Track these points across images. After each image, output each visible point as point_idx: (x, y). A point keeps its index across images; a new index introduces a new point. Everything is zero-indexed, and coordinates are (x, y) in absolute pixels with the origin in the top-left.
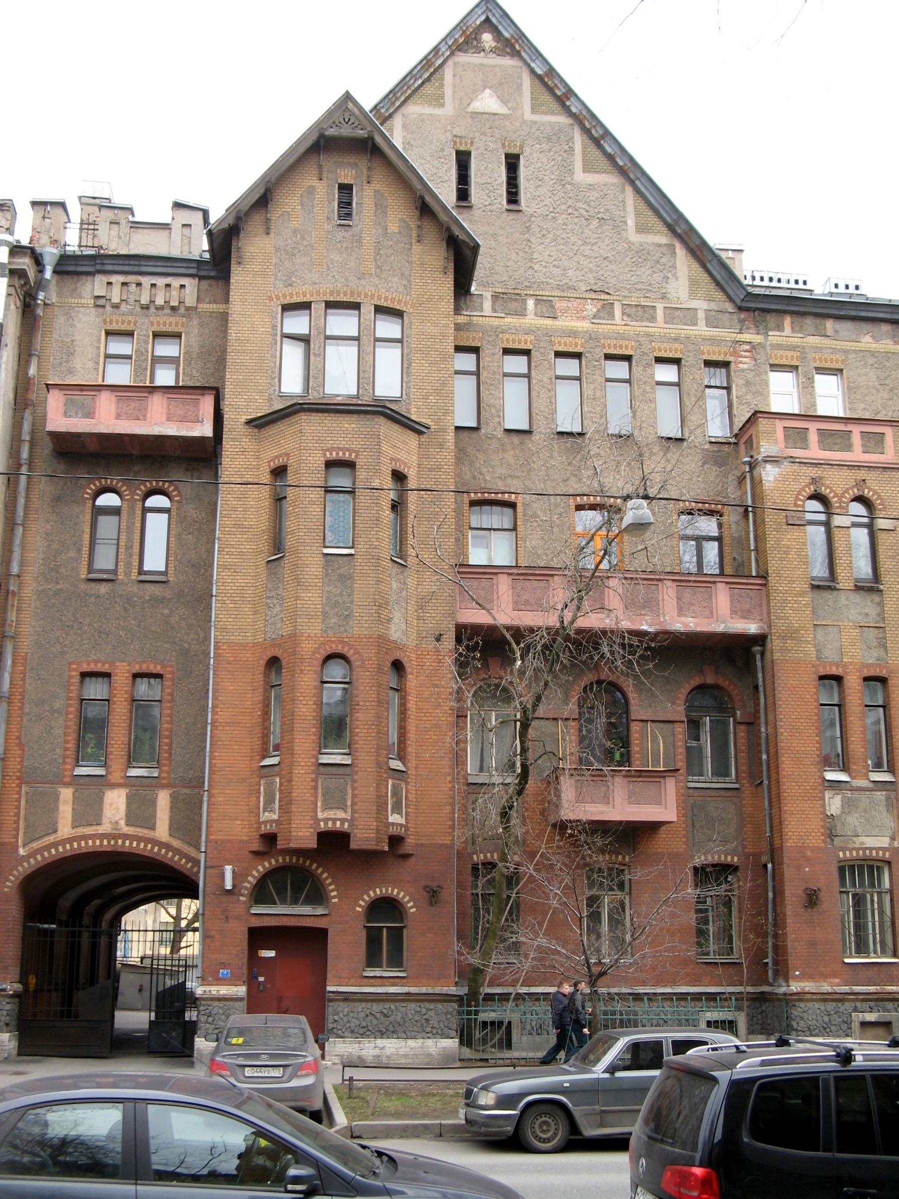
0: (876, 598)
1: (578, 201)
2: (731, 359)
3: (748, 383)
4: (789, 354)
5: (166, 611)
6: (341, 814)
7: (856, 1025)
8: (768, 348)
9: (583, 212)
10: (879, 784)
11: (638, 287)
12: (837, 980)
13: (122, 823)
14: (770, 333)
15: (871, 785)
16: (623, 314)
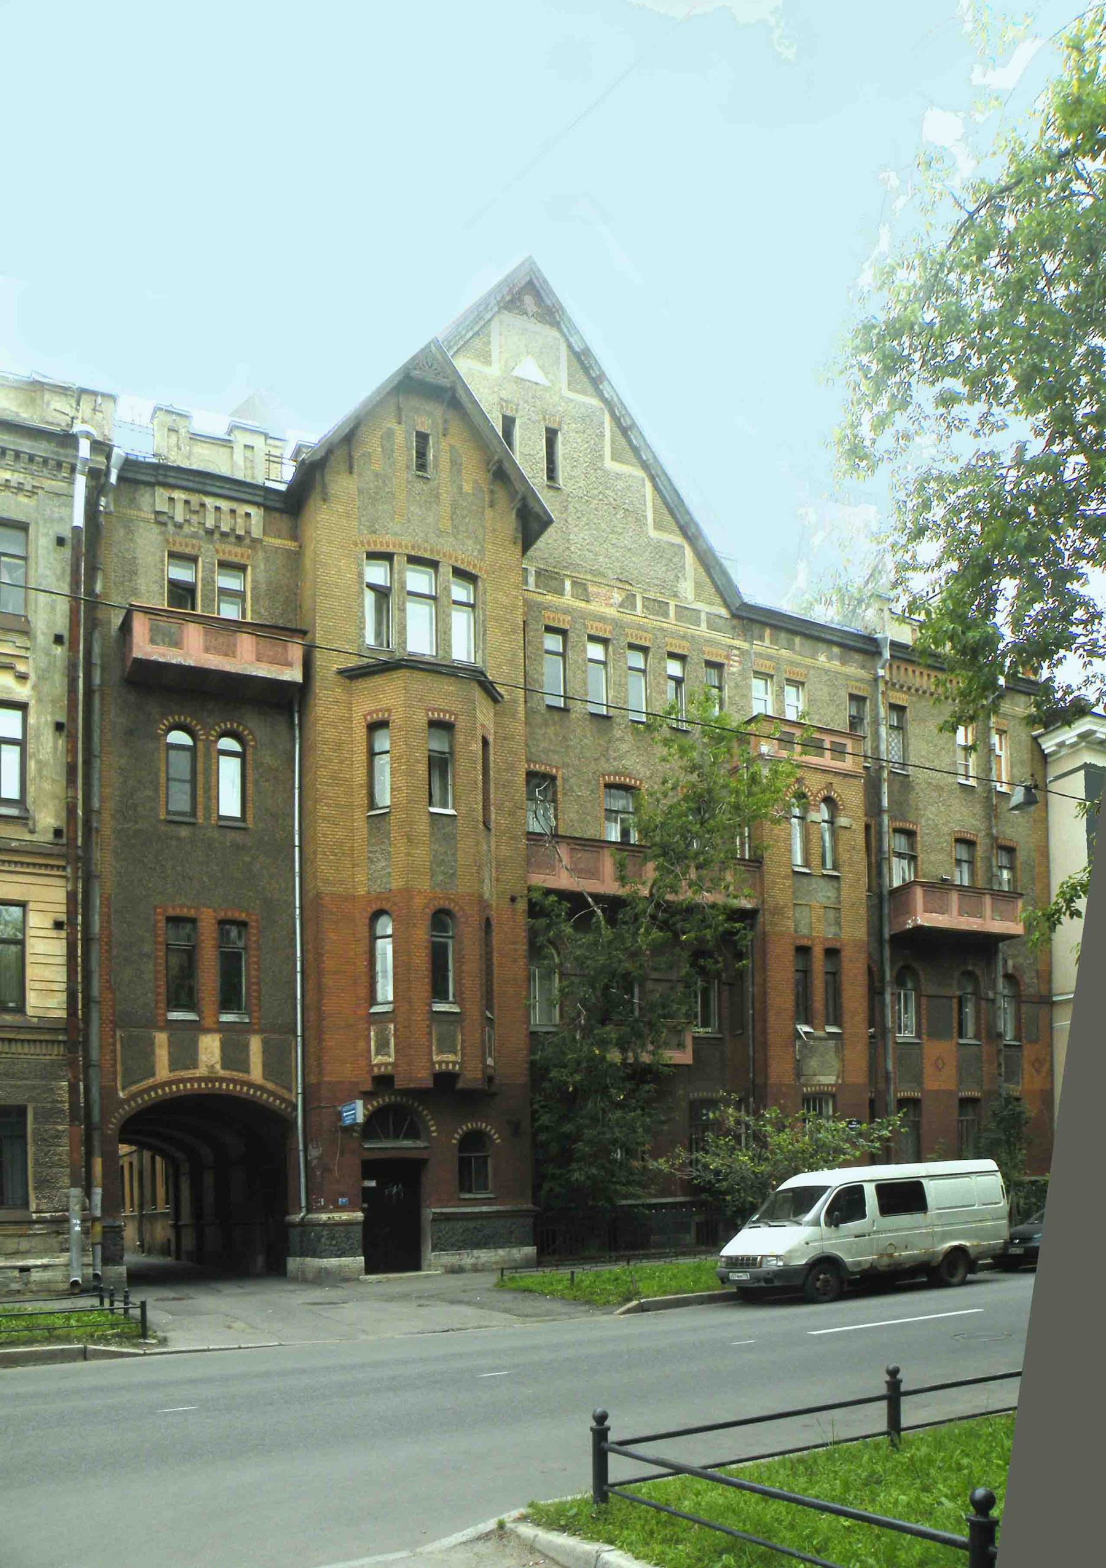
0: (836, 884)
2: (725, 661)
4: (768, 663)
5: (247, 859)
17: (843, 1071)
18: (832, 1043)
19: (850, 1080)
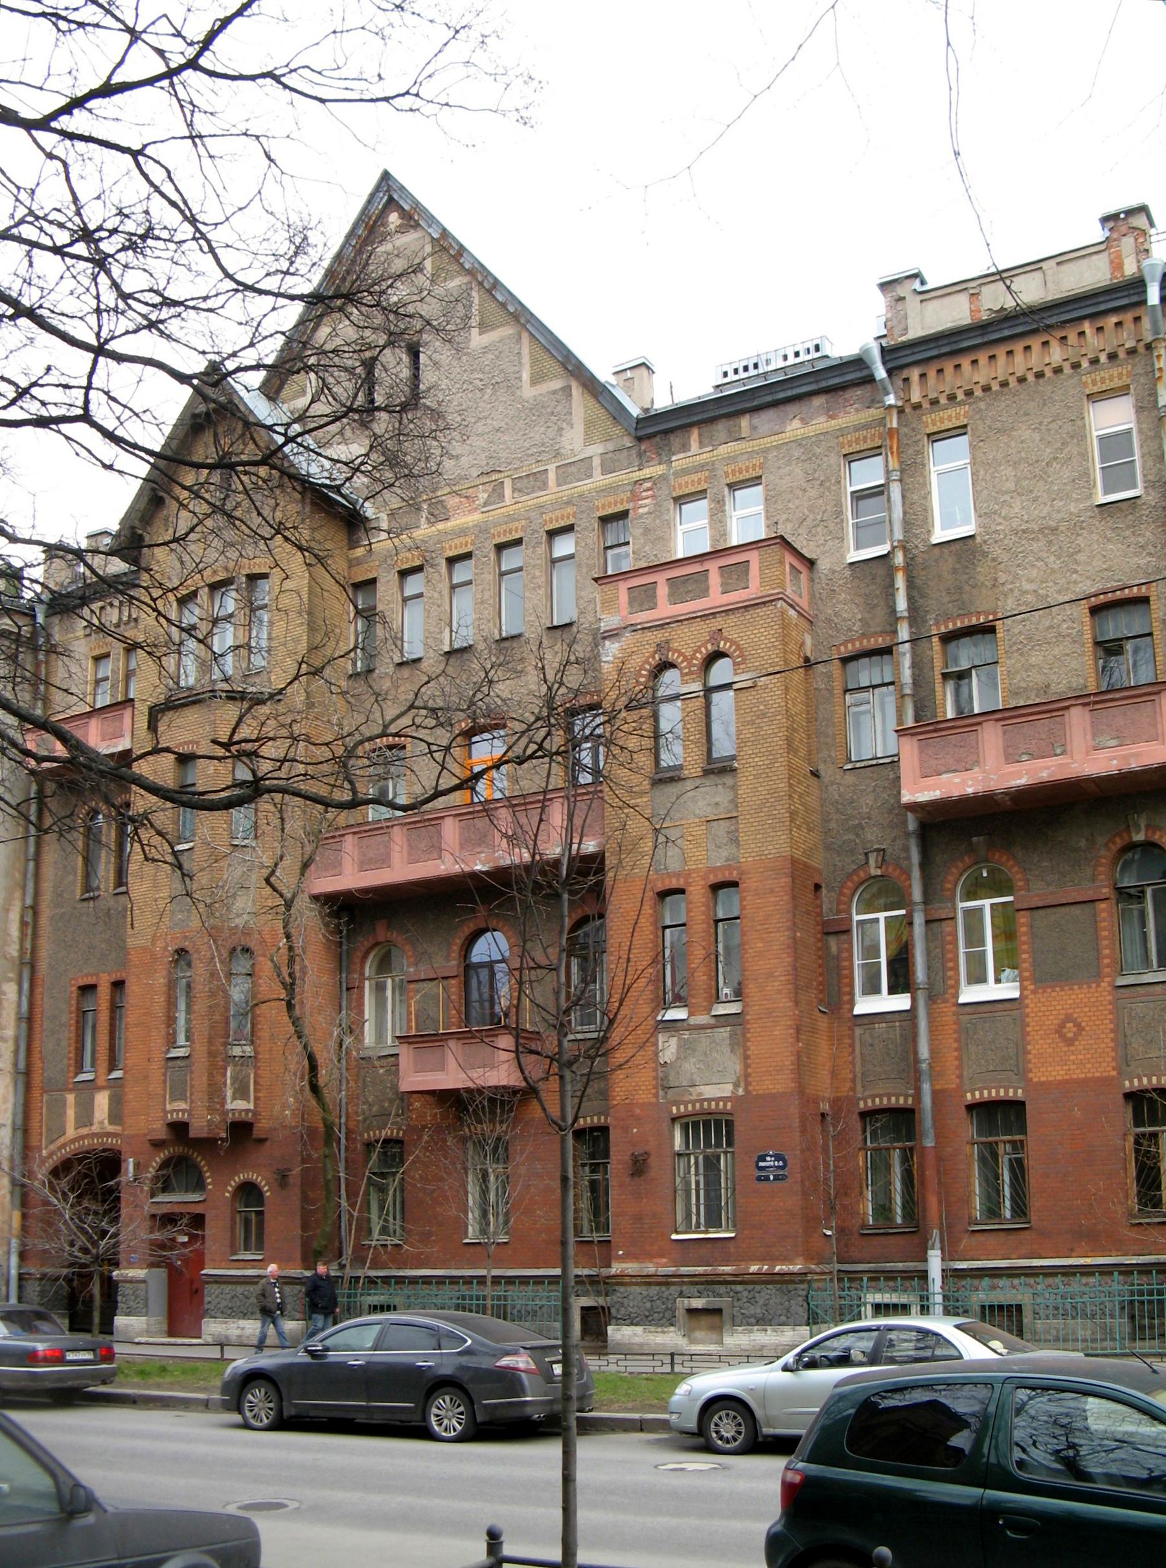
1: (472, 371)
3: (647, 531)
4: (695, 477)
6: (183, 1105)
7: (680, 1313)
8: (672, 477)
9: (477, 382)
10: (722, 1019)
11: (530, 452)
12: (664, 1260)
13: (106, 1122)
14: (674, 458)
15: (713, 1021)
16: (514, 490)
17: (747, 1076)
18: (724, 1033)
19: (757, 1088)
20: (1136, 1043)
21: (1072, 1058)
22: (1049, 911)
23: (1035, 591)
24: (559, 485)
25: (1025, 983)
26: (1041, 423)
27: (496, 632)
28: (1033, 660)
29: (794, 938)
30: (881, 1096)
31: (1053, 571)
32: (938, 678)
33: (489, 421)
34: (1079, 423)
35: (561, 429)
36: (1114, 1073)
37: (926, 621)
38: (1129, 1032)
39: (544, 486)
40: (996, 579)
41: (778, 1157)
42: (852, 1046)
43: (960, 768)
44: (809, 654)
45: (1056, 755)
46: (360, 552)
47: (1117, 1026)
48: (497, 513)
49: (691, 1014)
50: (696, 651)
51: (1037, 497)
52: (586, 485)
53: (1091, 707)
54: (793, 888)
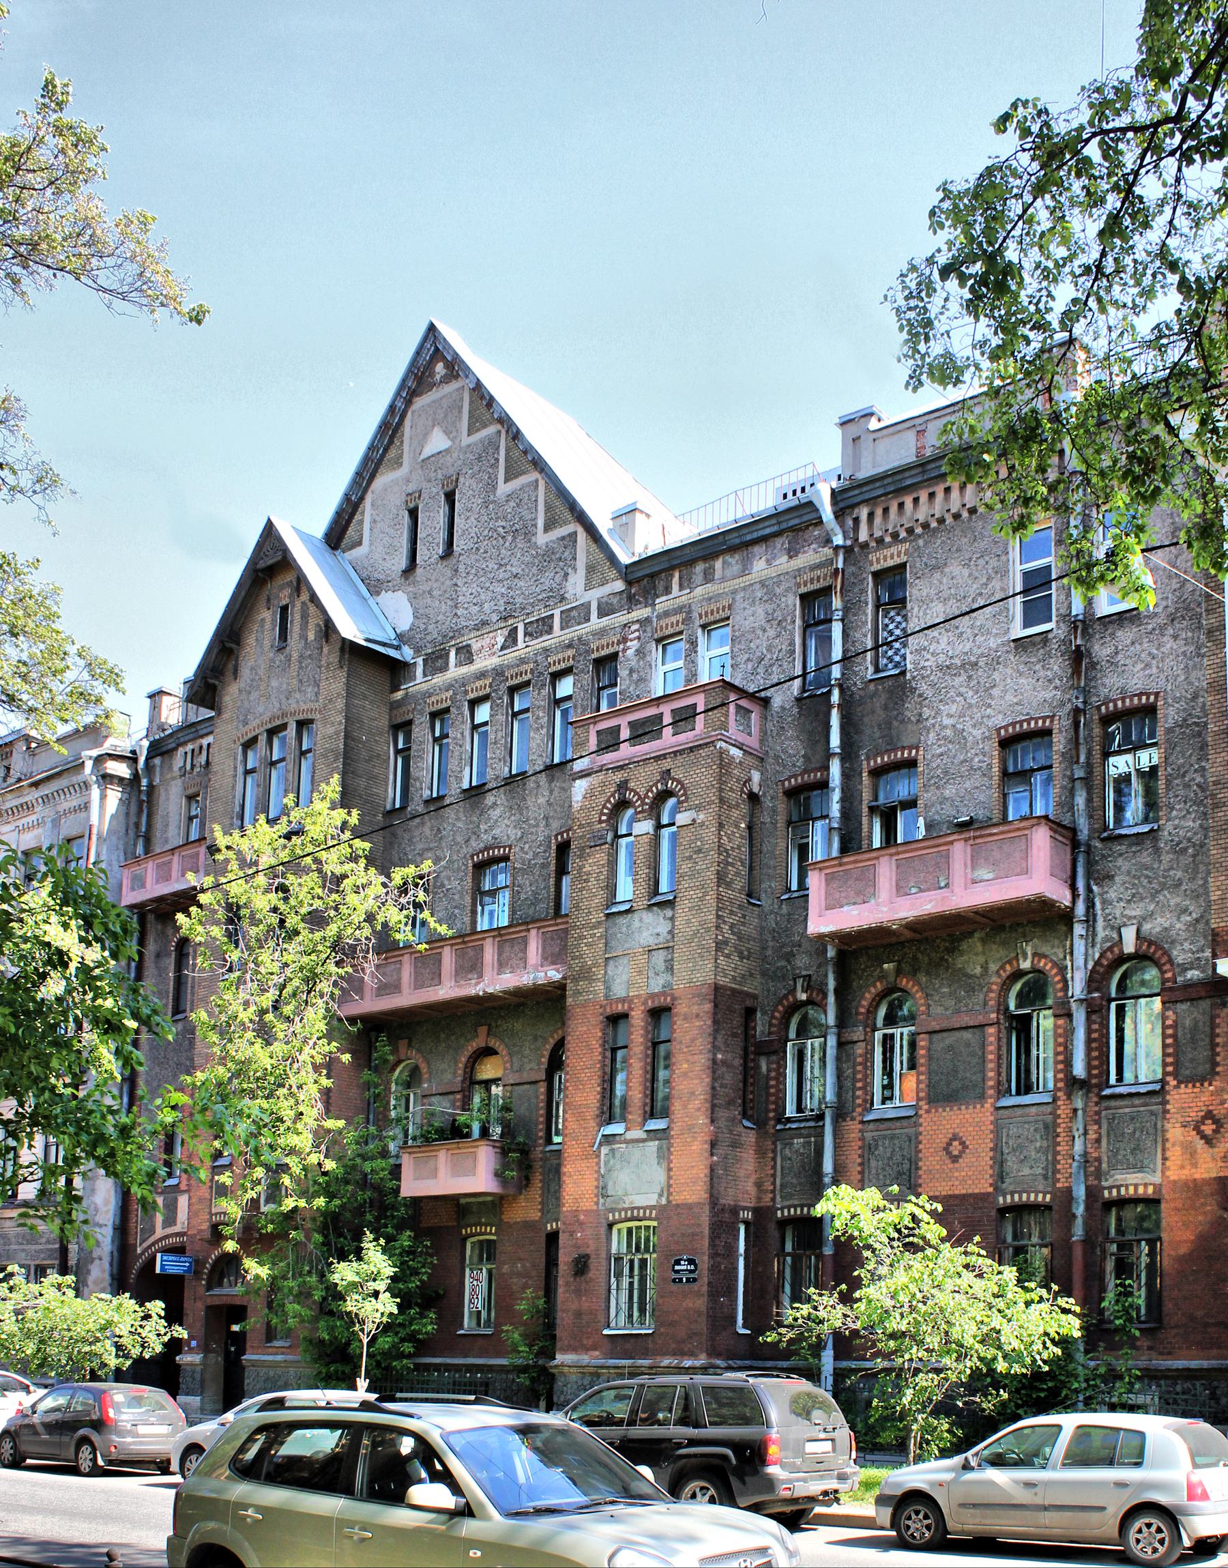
0: (669, 913)
4: (673, 619)
8: (655, 620)
9: (500, 529)
11: (540, 597)
14: (658, 601)
15: (644, 1136)
16: (526, 634)
17: (669, 1186)
19: (677, 1198)
20: (1011, 1163)
21: (956, 1174)
22: (945, 1034)
23: (954, 726)
24: (562, 629)
25: (921, 1103)
26: (970, 560)
27: (507, 769)
28: (947, 793)
29: (714, 1061)
30: (795, 1207)
31: (970, 706)
32: (865, 810)
33: (509, 567)
34: (1003, 558)
35: (566, 575)
36: (991, 1190)
37: (859, 756)
38: (1006, 1151)
39: (550, 630)
40: (920, 715)
41: (691, 1262)
42: (774, 1159)
43: (859, 900)
44: (756, 789)
45: (941, 888)
46: (399, 695)
47: (996, 1145)
48: (511, 655)
49: (627, 1129)
50: (648, 791)
51: (962, 633)
52: (582, 630)
53: (971, 842)
54: (715, 1014)
